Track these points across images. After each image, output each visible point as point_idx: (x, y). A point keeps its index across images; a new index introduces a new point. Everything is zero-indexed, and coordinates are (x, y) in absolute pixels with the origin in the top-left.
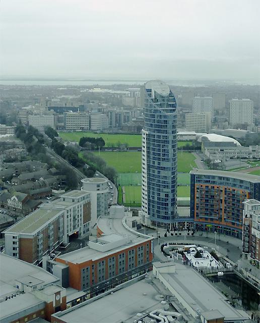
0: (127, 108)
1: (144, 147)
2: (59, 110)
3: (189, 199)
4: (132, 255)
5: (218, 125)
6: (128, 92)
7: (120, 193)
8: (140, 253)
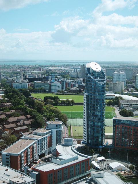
0: (73, 78)
1: (85, 103)
2: (31, 80)
3: (112, 134)
4: (78, 167)
5: (129, 90)
6: (73, 69)
7: (70, 131)
8: (82, 166)
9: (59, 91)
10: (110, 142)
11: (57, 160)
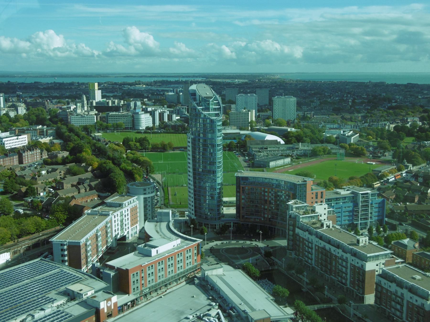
3: (234, 199)
9: (147, 128)
10: (232, 211)
11: (146, 248)
